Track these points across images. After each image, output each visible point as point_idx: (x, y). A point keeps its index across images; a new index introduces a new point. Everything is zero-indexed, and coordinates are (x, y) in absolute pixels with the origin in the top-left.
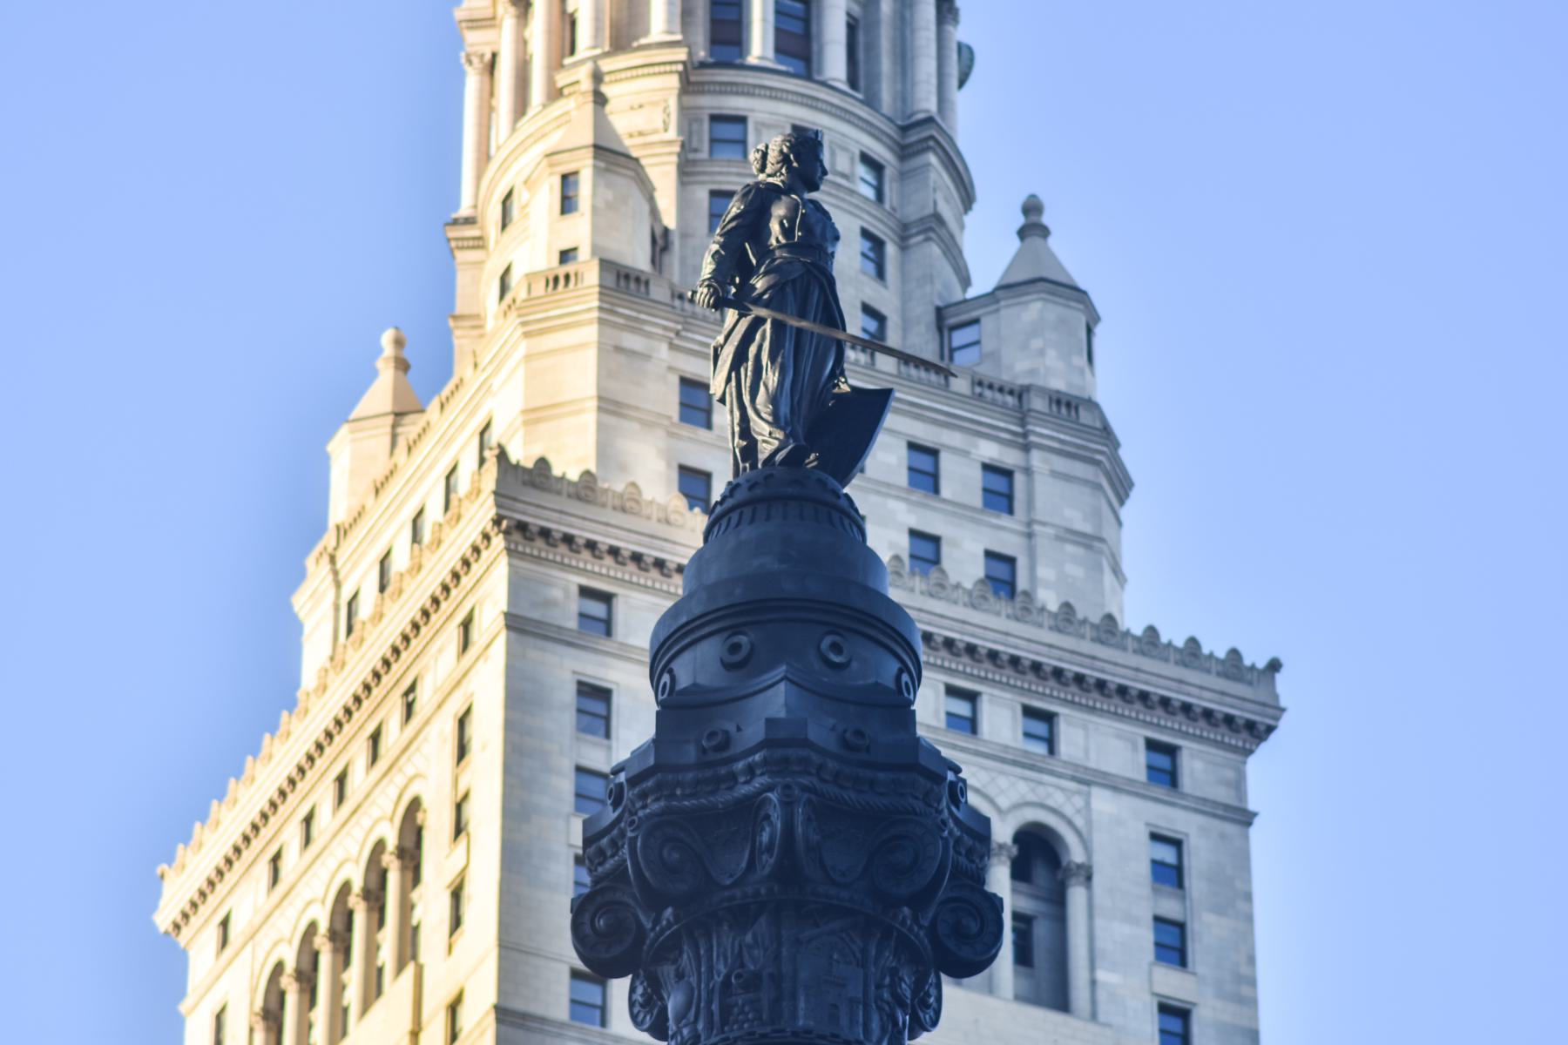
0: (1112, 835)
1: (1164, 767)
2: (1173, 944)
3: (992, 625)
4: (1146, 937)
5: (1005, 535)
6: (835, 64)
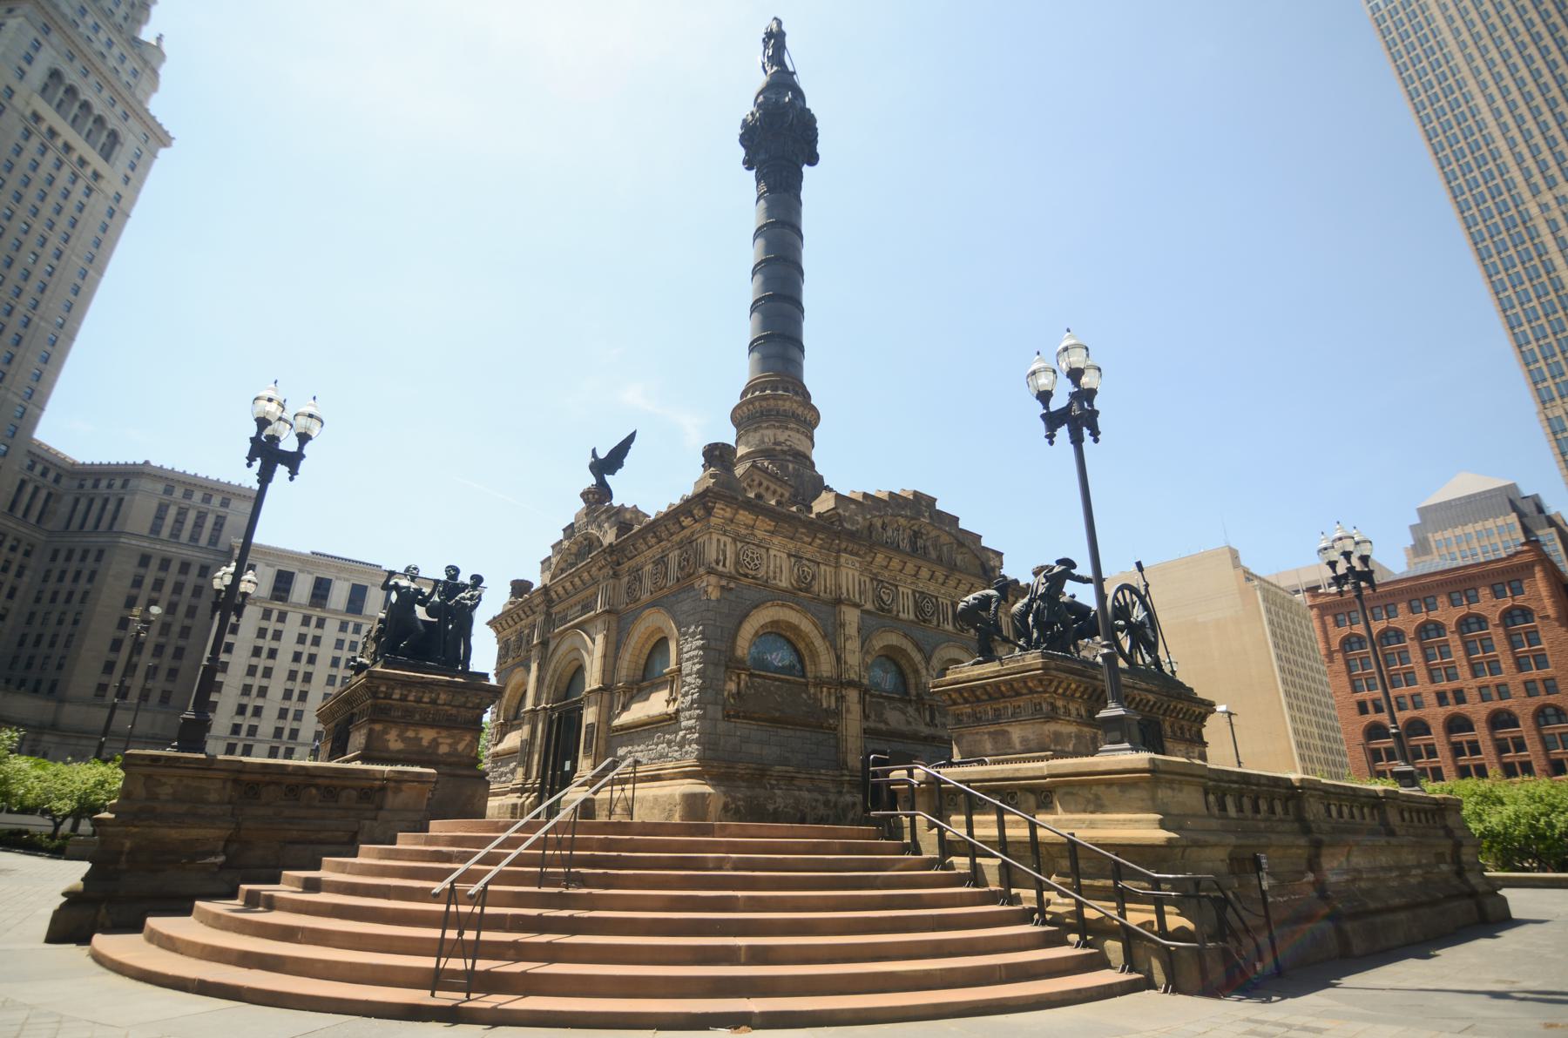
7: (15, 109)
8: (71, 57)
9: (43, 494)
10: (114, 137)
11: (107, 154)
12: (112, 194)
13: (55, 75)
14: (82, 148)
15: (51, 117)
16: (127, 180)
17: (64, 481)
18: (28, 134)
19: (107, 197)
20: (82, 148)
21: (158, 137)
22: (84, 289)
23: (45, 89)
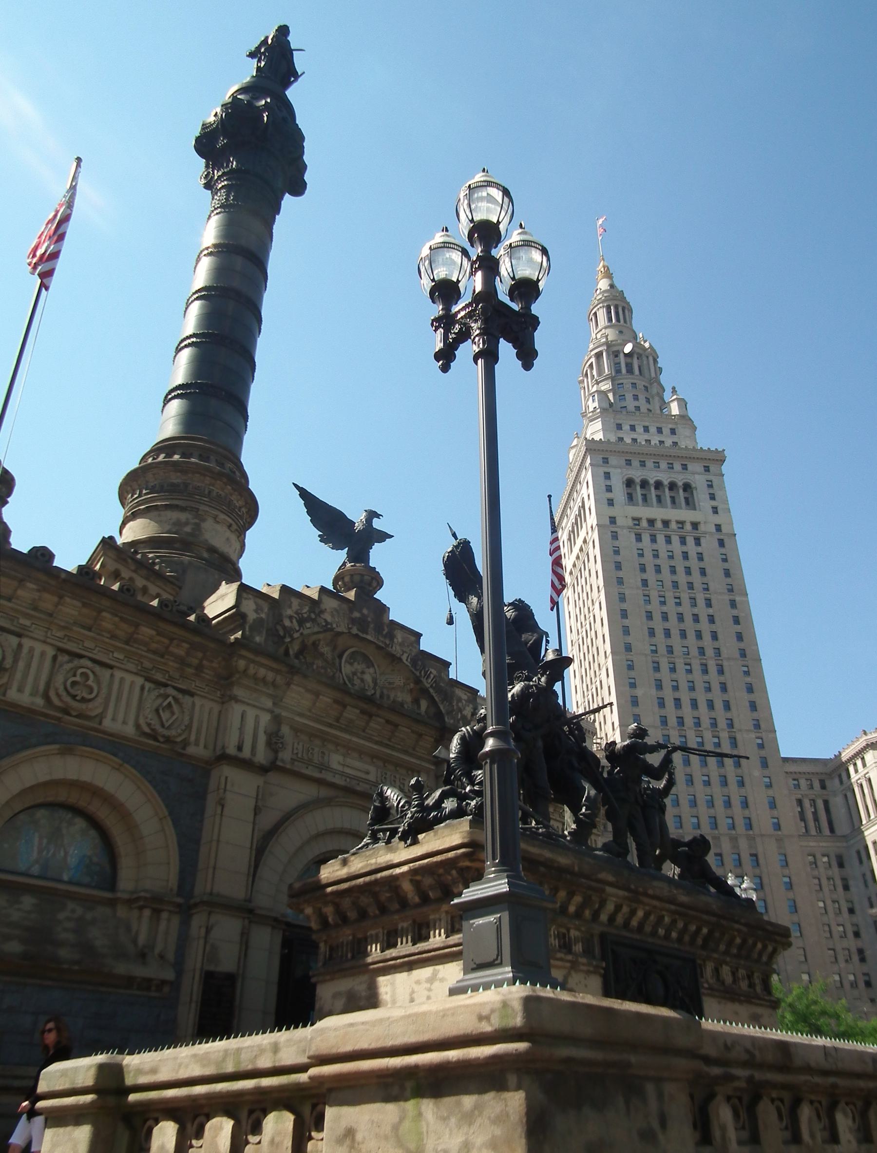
0: (699, 481)
1: (707, 469)
2: (712, 497)
3: (674, 452)
4: (708, 496)
5: (675, 439)
6: (637, 371)
7: (622, 527)
8: (629, 463)
9: (820, 804)
10: (687, 487)
11: (690, 503)
12: (713, 529)
13: (629, 483)
14: (674, 514)
15: (645, 512)
16: (715, 510)
17: (828, 783)
18: (639, 538)
19: (711, 534)
20: (674, 514)
21: (713, 461)
22: (742, 615)
23: (630, 497)
